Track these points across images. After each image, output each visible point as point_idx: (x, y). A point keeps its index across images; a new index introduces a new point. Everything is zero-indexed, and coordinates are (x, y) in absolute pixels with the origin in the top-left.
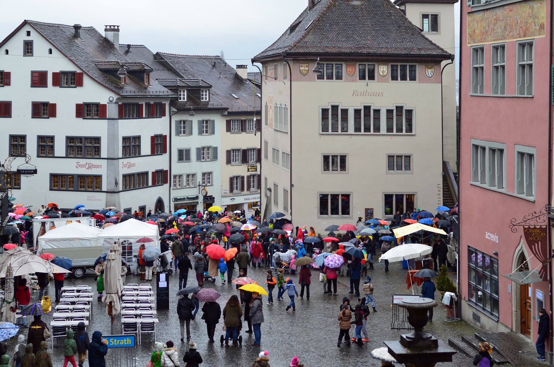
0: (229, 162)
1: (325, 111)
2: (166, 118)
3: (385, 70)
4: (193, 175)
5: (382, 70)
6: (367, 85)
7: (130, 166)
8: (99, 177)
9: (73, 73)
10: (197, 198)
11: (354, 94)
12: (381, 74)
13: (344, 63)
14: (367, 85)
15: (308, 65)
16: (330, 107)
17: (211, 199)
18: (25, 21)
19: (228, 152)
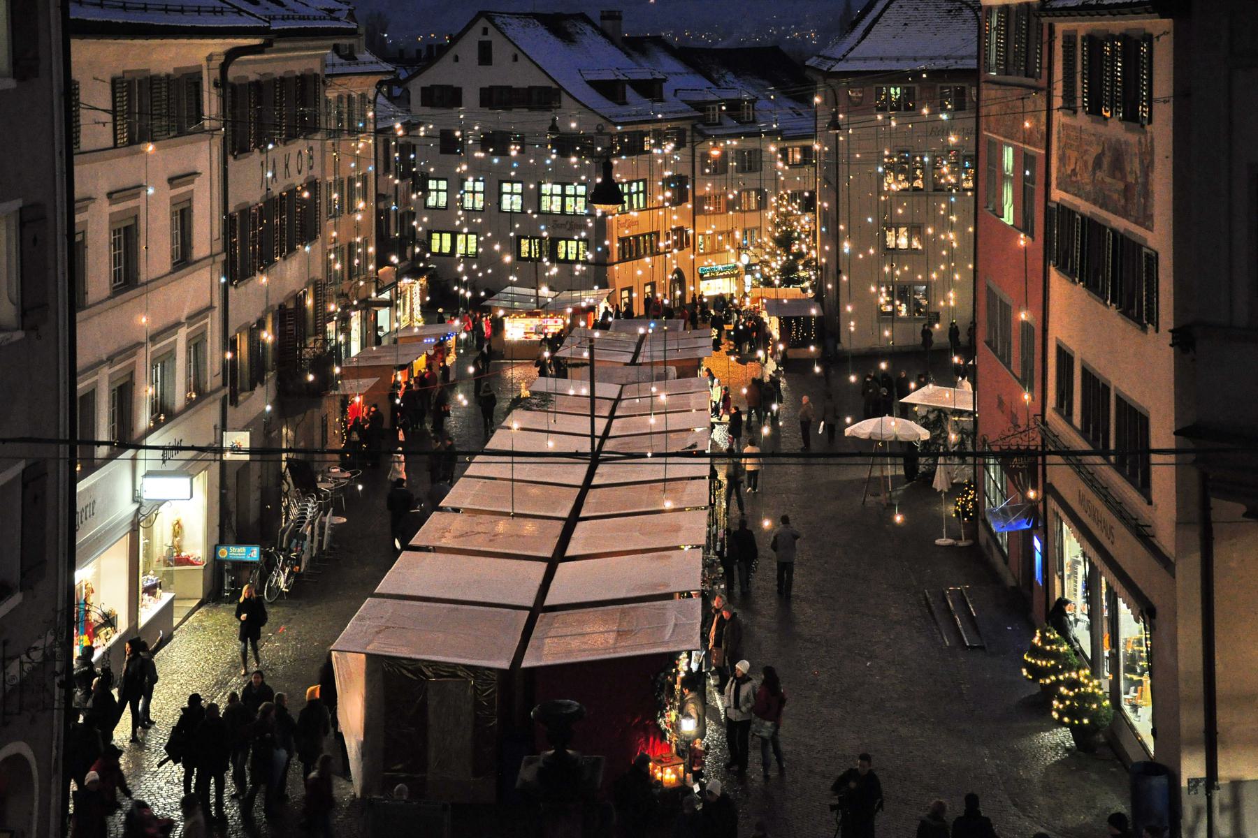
9: (546, 90)
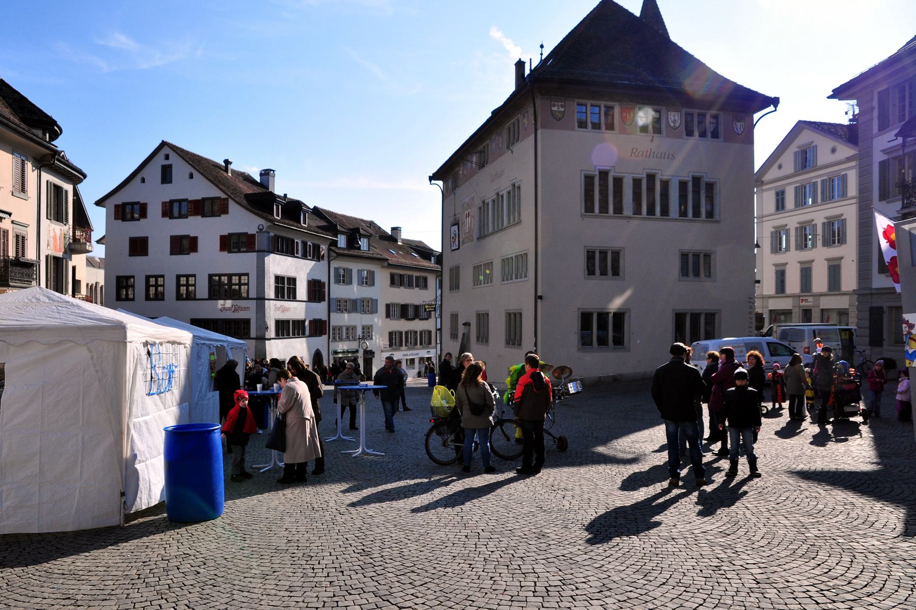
0: (388, 315)
1: (589, 180)
2: (324, 263)
3: (677, 119)
4: (354, 328)
5: (673, 119)
6: (652, 141)
7: (284, 310)
8: (247, 322)
10: (357, 351)
11: (633, 154)
12: (672, 124)
13: (617, 104)
14: (652, 141)
15: (563, 103)
16: (597, 173)
17: (371, 353)
18: (163, 141)
19: (388, 306)
